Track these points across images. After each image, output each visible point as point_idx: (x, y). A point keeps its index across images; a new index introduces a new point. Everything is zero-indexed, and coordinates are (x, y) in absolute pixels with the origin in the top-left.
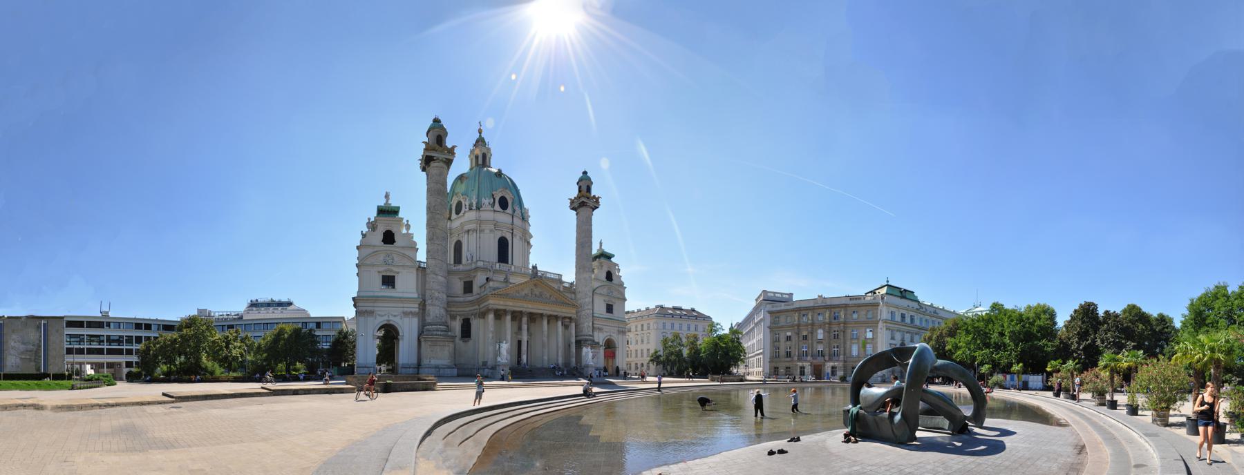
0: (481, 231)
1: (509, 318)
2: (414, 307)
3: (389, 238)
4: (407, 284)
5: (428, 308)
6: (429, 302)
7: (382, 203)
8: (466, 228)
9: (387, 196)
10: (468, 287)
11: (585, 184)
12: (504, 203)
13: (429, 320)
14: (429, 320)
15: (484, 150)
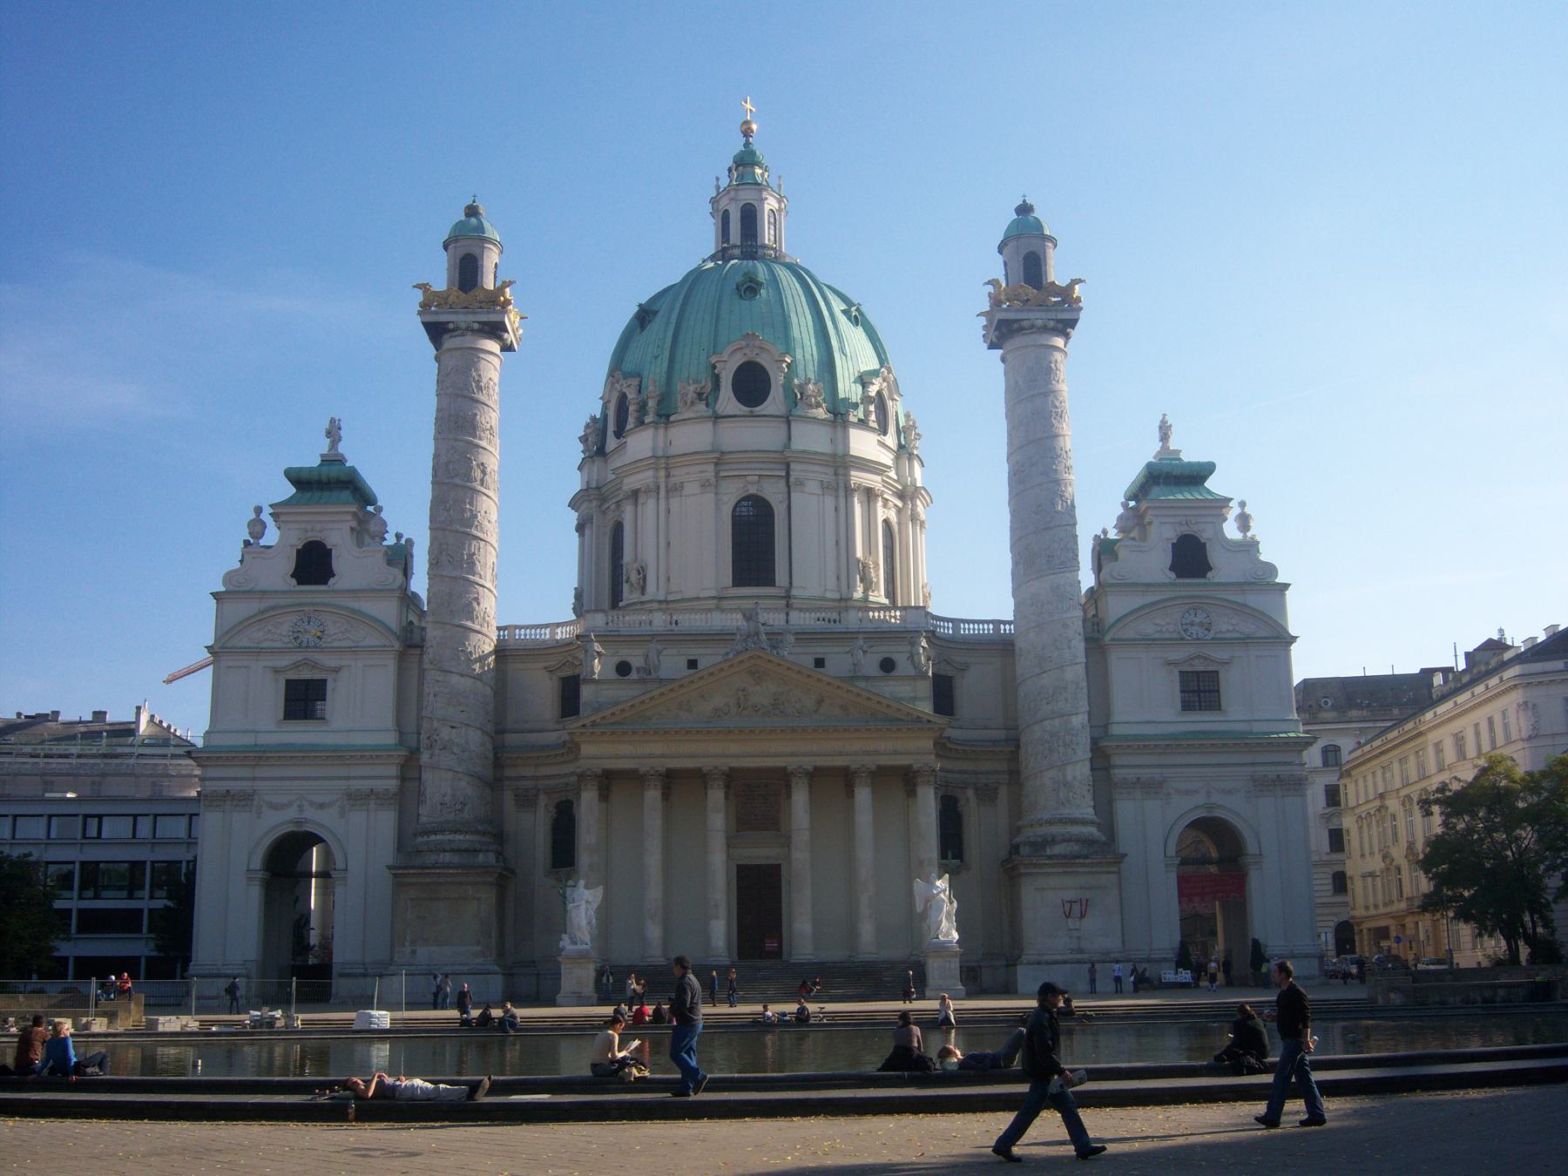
0: (674, 490)
1: (653, 795)
2: (386, 778)
3: (313, 564)
4: (362, 706)
5: (424, 776)
6: (425, 757)
7: (310, 459)
8: (631, 483)
9: (334, 432)
10: (570, 694)
11: (1026, 247)
12: (752, 384)
13: (426, 814)
14: (426, 814)
15: (747, 196)
